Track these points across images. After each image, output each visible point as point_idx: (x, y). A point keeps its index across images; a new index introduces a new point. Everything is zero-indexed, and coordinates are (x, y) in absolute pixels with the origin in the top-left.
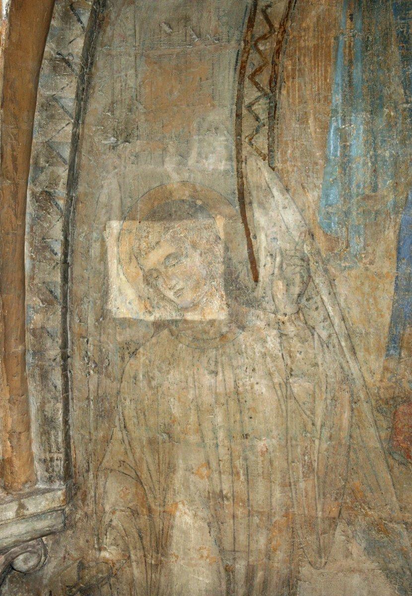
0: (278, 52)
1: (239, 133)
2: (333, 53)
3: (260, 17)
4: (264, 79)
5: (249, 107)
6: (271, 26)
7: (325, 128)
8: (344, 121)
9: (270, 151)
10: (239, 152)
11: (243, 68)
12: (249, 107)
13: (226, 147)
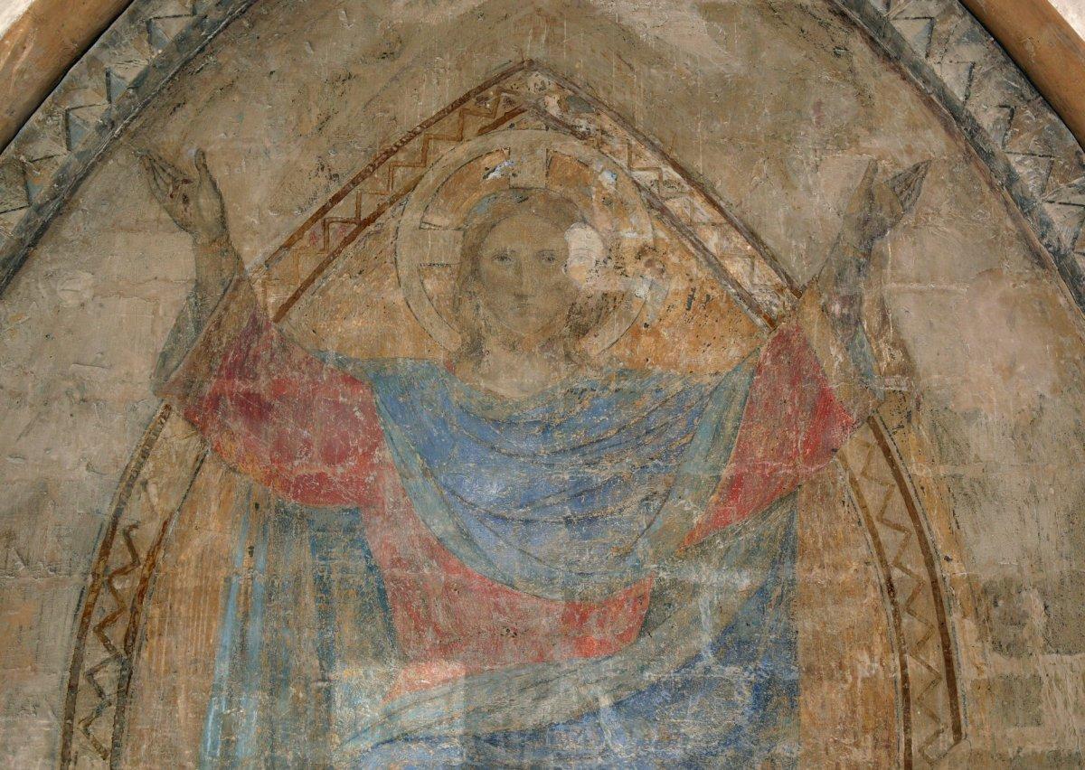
0: (141, 594)
1: (70, 716)
2: (221, 601)
3: (120, 541)
4: (117, 633)
5: (91, 674)
6: (135, 555)
7: (201, 714)
8: (230, 703)
9: (115, 745)
10: (66, 746)
11: (87, 614)
12: (91, 674)
13: (48, 735)
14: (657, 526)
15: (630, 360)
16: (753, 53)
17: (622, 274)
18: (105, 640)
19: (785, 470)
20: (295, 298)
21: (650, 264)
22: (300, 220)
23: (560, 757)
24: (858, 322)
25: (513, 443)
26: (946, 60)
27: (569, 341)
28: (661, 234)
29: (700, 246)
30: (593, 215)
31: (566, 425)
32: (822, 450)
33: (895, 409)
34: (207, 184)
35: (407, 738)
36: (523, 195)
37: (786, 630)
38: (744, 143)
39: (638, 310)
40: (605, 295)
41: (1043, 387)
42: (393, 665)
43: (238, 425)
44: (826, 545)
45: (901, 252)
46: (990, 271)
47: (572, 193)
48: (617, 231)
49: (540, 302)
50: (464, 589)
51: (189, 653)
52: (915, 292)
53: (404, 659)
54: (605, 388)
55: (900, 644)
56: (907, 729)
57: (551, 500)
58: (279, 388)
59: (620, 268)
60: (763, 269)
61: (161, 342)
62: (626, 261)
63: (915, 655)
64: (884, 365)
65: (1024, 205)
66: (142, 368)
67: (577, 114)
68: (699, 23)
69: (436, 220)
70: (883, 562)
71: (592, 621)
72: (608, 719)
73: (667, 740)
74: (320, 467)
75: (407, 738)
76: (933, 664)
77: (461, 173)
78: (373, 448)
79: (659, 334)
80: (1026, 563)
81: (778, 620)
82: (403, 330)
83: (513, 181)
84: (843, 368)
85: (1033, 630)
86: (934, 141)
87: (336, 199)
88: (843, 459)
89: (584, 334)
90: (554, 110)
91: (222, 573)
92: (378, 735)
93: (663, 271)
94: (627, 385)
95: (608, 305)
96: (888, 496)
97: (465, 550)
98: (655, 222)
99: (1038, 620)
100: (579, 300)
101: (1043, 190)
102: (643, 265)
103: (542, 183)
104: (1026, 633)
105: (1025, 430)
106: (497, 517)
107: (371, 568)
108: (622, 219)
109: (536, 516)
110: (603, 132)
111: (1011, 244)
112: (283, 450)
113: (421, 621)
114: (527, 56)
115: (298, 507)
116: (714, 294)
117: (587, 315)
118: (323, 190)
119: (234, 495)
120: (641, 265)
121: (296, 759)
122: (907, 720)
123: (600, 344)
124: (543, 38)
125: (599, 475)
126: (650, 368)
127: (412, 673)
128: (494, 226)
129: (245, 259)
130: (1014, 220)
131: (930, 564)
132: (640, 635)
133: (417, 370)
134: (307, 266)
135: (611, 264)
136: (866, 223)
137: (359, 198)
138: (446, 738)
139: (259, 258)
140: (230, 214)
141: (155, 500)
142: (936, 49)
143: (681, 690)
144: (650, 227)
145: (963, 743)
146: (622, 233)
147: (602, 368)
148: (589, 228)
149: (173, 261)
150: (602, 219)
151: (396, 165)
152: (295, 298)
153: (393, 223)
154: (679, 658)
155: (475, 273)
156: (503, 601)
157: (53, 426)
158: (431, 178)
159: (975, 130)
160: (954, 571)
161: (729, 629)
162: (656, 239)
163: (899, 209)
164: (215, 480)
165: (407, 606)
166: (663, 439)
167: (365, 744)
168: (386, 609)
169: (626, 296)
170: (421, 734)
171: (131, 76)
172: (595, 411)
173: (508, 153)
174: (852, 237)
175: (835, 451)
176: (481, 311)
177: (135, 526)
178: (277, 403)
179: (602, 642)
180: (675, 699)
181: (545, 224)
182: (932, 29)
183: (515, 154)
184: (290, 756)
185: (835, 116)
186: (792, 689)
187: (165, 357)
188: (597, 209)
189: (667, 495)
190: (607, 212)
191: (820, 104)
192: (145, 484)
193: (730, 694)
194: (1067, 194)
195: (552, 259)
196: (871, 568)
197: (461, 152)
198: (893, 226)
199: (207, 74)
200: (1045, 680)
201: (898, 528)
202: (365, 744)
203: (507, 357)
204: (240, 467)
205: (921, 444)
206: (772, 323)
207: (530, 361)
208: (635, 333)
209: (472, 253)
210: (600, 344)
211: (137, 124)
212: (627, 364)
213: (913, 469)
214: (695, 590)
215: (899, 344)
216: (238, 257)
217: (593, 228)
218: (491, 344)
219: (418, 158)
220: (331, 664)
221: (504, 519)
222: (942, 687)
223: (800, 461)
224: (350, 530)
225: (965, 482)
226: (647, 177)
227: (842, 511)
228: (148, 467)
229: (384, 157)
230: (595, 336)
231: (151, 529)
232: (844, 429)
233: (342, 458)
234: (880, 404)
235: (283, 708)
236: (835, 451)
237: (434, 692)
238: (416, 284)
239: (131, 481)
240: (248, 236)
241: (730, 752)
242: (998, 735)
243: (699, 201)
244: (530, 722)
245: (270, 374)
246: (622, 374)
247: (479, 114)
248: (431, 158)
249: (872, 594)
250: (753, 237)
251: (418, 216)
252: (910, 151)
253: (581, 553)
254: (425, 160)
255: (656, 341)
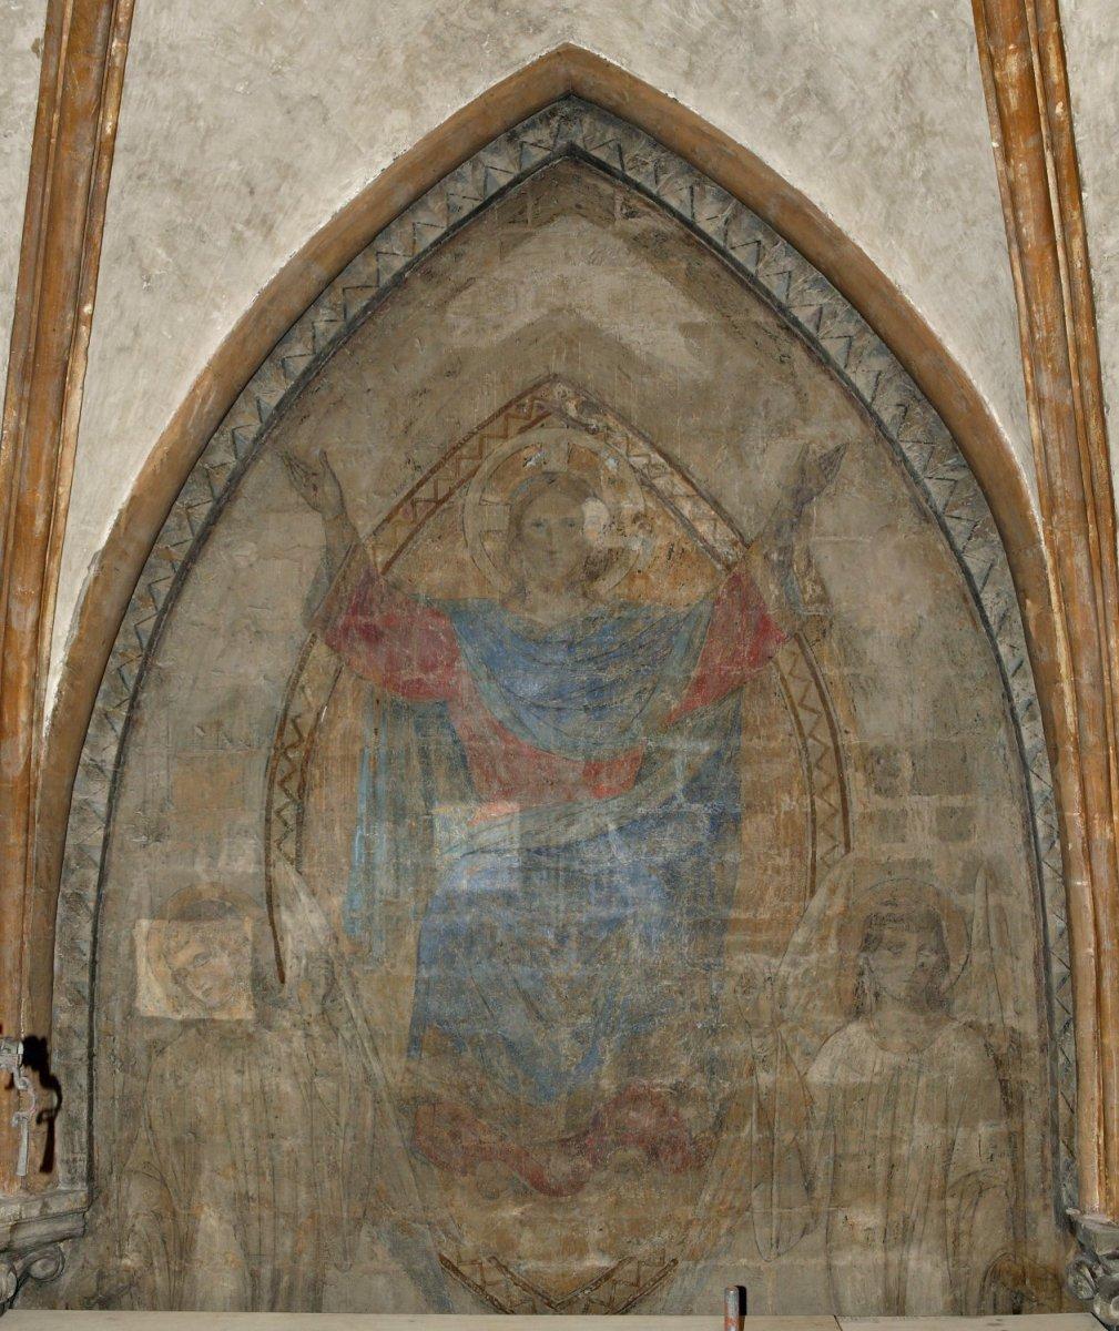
0: (307, 760)
1: (268, 837)
2: (358, 766)
3: (289, 727)
4: (293, 785)
5: (278, 813)
6: (300, 736)
7: (351, 836)
8: (368, 830)
9: (298, 856)
10: (267, 856)
11: (273, 774)
12: (278, 813)
13: (255, 850)
14: (646, 711)
16: (720, 360)
18: (286, 790)
19: (735, 672)
20: (395, 557)
21: (642, 526)
22: (395, 501)
23: (582, 862)
24: (790, 566)
25: (548, 656)
26: (860, 370)
28: (650, 504)
29: (678, 512)
31: (585, 644)
32: (761, 658)
33: (816, 626)
34: (329, 475)
35: (483, 851)
36: (551, 478)
37: (733, 780)
38: (710, 434)
41: (922, 610)
42: (473, 804)
43: (362, 647)
44: (763, 723)
45: (824, 514)
46: (888, 526)
47: (586, 476)
49: (567, 557)
50: (518, 754)
51: (338, 797)
52: (831, 542)
53: (480, 800)
54: (610, 616)
55: (811, 789)
56: (814, 845)
57: (574, 695)
58: (389, 620)
60: (722, 528)
61: (306, 590)
63: (821, 796)
64: (807, 597)
65: (912, 477)
66: (295, 609)
67: (590, 416)
68: (679, 339)
69: (491, 498)
70: (802, 735)
71: (603, 775)
72: (614, 838)
73: (653, 852)
74: (418, 675)
75: (483, 851)
76: (832, 802)
77: (510, 462)
78: (453, 661)
80: (901, 734)
81: (729, 774)
82: (471, 578)
83: (545, 468)
84: (778, 599)
85: (903, 779)
86: (852, 428)
87: (420, 484)
88: (776, 663)
90: (573, 413)
91: (357, 747)
92: (464, 849)
94: (625, 614)
95: (612, 557)
96: (807, 689)
97: (517, 729)
99: (907, 773)
101: (925, 469)
103: (565, 468)
104: (898, 782)
105: (906, 643)
106: (538, 707)
107: (455, 742)
109: (565, 705)
110: (609, 428)
111: (905, 505)
112: (393, 663)
113: (490, 776)
114: (552, 370)
115: (404, 702)
116: (688, 548)
118: (409, 477)
119: (362, 694)
120: (636, 527)
121: (413, 864)
122: (814, 839)
124: (564, 355)
125: (607, 677)
127: (485, 809)
129: (359, 530)
130: (908, 487)
131: (834, 735)
132: (636, 783)
134: (402, 534)
135: (614, 527)
136: (798, 492)
137: (436, 483)
138: (509, 851)
139: (369, 529)
140: (347, 497)
141: (311, 699)
142: (853, 361)
143: (663, 820)
145: (851, 854)
149: (311, 532)
150: (608, 494)
151: (461, 458)
152: (395, 557)
153: (461, 501)
154: (660, 798)
155: (519, 537)
156: (543, 761)
157: (239, 650)
158: (486, 466)
159: (880, 424)
160: (850, 740)
161: (695, 779)
162: (646, 507)
163: (823, 482)
164: (349, 685)
165: (480, 766)
166: (651, 652)
167: (457, 855)
168: (466, 767)
169: (624, 550)
170: (491, 848)
171: (274, 403)
172: (604, 632)
173: (540, 447)
174: (787, 503)
175: (770, 658)
177: (299, 716)
178: (387, 631)
179: (610, 789)
180: (658, 825)
182: (850, 346)
183: (546, 447)
184: (409, 863)
185: (779, 411)
186: (737, 819)
187: (309, 601)
188: (604, 487)
189: (654, 689)
191: (768, 401)
192: (303, 688)
193: (693, 822)
194: (943, 472)
195: (573, 525)
196: (793, 738)
197: (506, 447)
198: (819, 493)
199: (323, 392)
200: (910, 813)
201: (813, 711)
202: (457, 855)
203: (542, 596)
204: (365, 675)
205: (831, 652)
206: (728, 568)
208: (631, 577)
209: (517, 522)
211: (276, 432)
213: (825, 671)
214: (672, 754)
215: (819, 581)
216: (355, 529)
218: (532, 587)
219: (476, 452)
220: (432, 803)
221: (543, 707)
222: (838, 820)
223: (745, 666)
224: (440, 716)
225: (862, 678)
226: (640, 462)
227: (774, 700)
228: (304, 677)
229: (451, 452)
231: (309, 719)
232: (778, 642)
233: (434, 667)
234: (804, 624)
235: (403, 832)
236: (770, 658)
237: (500, 821)
238: (478, 545)
239: (293, 686)
240: (361, 512)
241: (694, 859)
242: (875, 848)
243: (677, 479)
244: (563, 840)
245: (381, 612)
246: (622, 607)
247: (518, 418)
248: (486, 453)
249: (793, 756)
250: (716, 505)
251: (478, 495)
252: (833, 436)
253: (596, 729)
254: (481, 453)
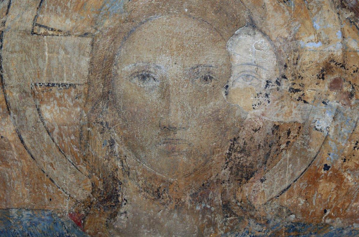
15: (304, 212)
17: (300, 99)
21: (336, 85)
27: (229, 187)
30: (264, 17)
39: (318, 147)
40: (276, 127)
48: (296, 39)
59: (297, 90)
62: (305, 81)
79: (342, 179)
89: (247, 179)
93: (351, 95)
98: (346, 27)
100: (243, 134)
102: (326, 88)
108: (303, 23)
117: (253, 154)
120: (324, 87)
123: (267, 191)
126: (328, 221)
128: (131, 32)
133: (36, 224)
135: (285, 85)
144: (339, 34)
146: (302, 43)
147: (268, 222)
148: (259, 35)
162: (346, 51)
169: (303, 128)
176: (116, 148)
181: (201, 30)
188: (270, 8)
190: (284, 11)
207: (179, 213)
210: (267, 191)
212: (300, 217)
217: (264, 34)
218: (131, 191)
230: (262, 181)
238: (30, 111)
251: (29, 15)
255: (338, 188)
